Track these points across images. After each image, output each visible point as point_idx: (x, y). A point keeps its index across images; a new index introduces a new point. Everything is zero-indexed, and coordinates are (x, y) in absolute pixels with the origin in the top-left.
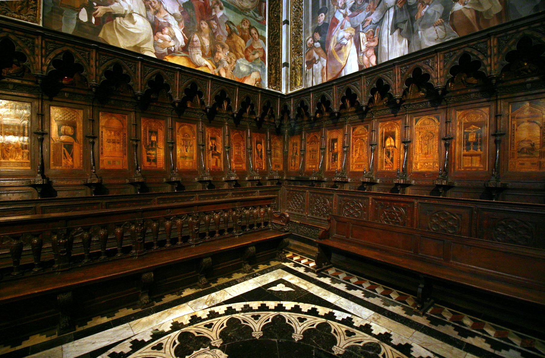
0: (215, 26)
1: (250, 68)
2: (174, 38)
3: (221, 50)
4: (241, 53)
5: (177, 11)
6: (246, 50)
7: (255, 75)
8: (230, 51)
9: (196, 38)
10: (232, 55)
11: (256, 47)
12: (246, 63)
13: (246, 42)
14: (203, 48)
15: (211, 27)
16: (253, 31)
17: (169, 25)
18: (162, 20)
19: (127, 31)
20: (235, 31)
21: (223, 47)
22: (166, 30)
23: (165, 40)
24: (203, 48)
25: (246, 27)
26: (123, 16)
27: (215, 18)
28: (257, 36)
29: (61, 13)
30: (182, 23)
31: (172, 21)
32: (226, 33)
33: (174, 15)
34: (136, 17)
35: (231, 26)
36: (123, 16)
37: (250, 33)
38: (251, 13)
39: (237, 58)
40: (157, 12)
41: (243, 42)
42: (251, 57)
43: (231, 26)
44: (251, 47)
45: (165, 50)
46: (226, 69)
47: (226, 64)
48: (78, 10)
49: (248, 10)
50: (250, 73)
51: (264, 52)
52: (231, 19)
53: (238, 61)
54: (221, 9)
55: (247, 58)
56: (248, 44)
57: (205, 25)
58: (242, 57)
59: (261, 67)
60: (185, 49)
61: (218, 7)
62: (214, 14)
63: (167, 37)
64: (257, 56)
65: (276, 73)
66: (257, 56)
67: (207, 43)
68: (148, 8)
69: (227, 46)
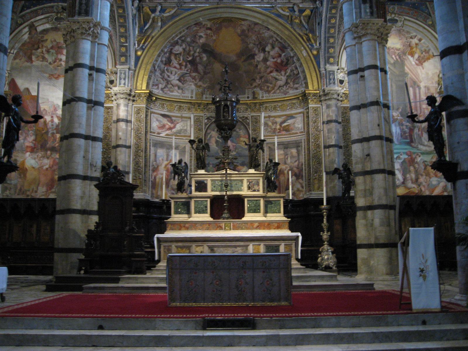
8: (426, 176)
15: (415, 168)
43: (426, 163)
46: (424, 186)
50: (439, 184)
54: (420, 156)
57: (412, 168)
62: (416, 161)
67: (413, 176)
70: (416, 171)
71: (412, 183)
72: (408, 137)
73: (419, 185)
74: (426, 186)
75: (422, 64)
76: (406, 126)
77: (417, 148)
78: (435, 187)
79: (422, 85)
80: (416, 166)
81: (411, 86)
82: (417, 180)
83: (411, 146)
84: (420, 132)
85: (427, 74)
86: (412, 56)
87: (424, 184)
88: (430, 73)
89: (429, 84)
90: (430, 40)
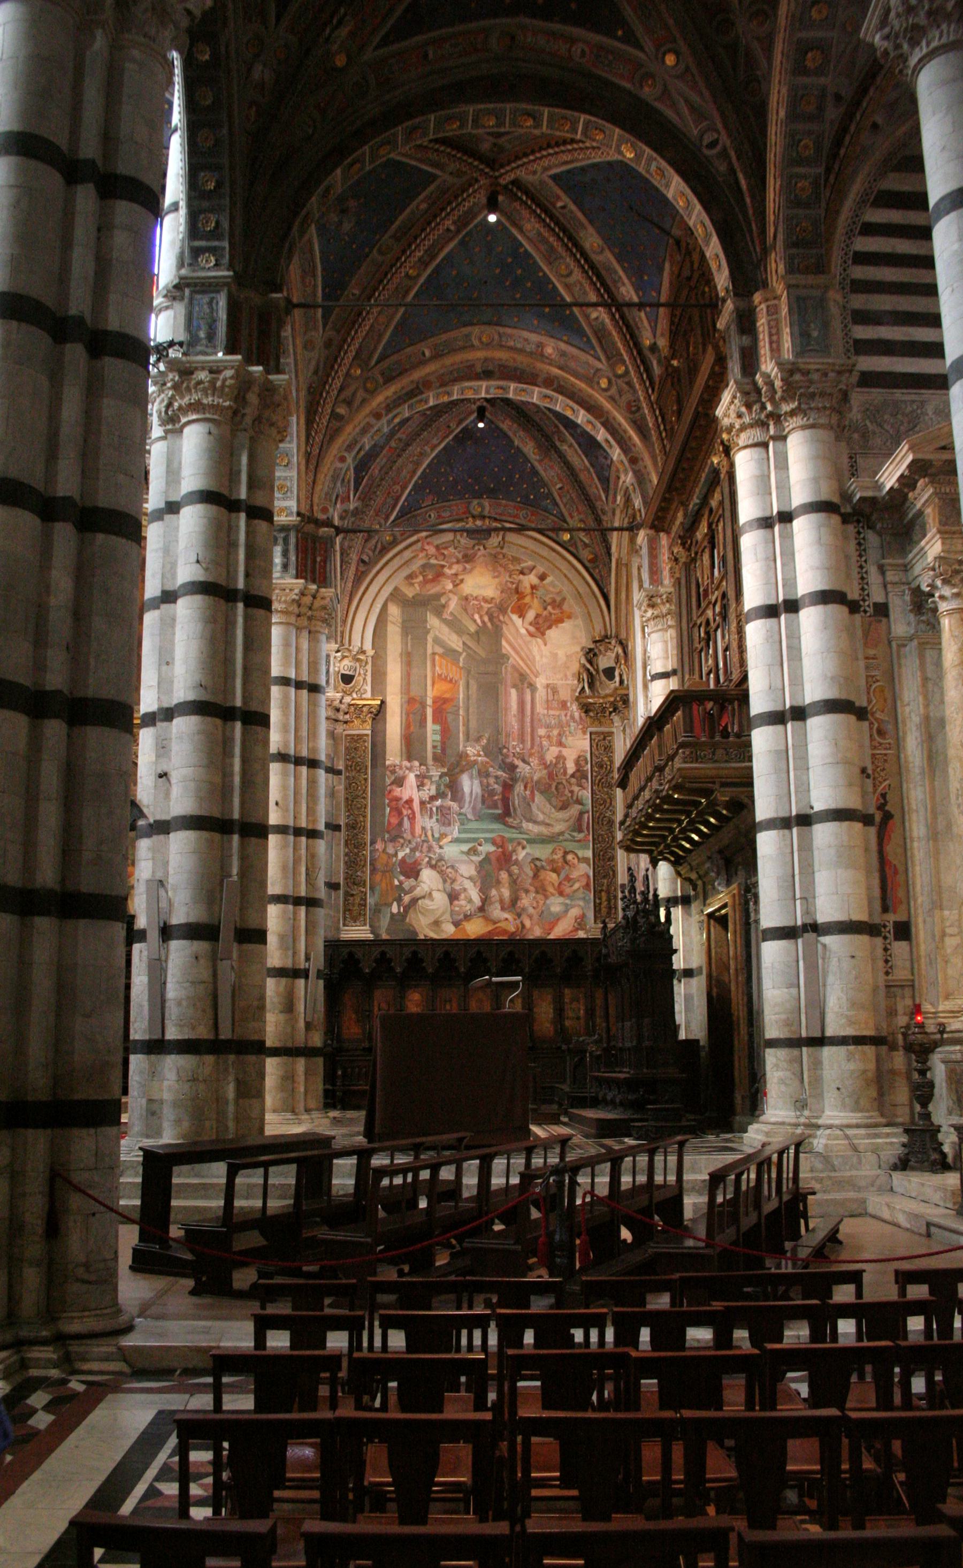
0: (516, 871)
1: (566, 905)
2: (470, 901)
3: (524, 895)
4: (551, 889)
5: (473, 872)
6: (560, 883)
7: (574, 912)
8: (537, 892)
9: (494, 892)
10: (539, 897)
11: (575, 875)
12: (561, 900)
13: (558, 875)
14: (501, 901)
15: (510, 874)
16: (570, 857)
17: (465, 890)
18: (457, 888)
19: (427, 910)
20: (543, 867)
21: (527, 891)
22: (462, 896)
23: (461, 906)
24: (501, 901)
25: (558, 856)
26: (424, 897)
27: (516, 862)
28: (576, 861)
29: (379, 911)
30: (478, 884)
31: (468, 884)
32: (531, 874)
33: (470, 878)
34: (435, 894)
35: (538, 863)
36: (424, 897)
37: (566, 862)
38: (567, 836)
39: (546, 897)
40: (453, 881)
41: (554, 875)
42: (568, 890)
43: (538, 863)
44: (568, 879)
45: (462, 917)
46: (530, 917)
47: (531, 910)
48: (391, 905)
49: (562, 833)
50: (566, 911)
51: (588, 877)
52: (537, 855)
53: (548, 902)
54: (524, 848)
55: (561, 894)
56: (563, 875)
57: (504, 875)
58: (553, 895)
59: (584, 898)
60: (481, 909)
61: (520, 848)
63: (463, 903)
64: (577, 886)
65: (609, 900)
66: (577, 886)
67: (506, 893)
68: (445, 881)
69: (532, 888)
70: (514, 882)
71: (503, 909)
72: (500, 804)
73: (519, 915)
74: (536, 917)
75: (543, 634)
76: (497, 777)
77: (518, 828)
78: (557, 919)
79: (540, 682)
80: (515, 869)
81: (515, 686)
82: (514, 901)
83: (506, 824)
84: (528, 793)
85: (555, 656)
86: (522, 615)
87: (531, 910)
88: (561, 653)
89: (557, 680)
90: (565, 576)
